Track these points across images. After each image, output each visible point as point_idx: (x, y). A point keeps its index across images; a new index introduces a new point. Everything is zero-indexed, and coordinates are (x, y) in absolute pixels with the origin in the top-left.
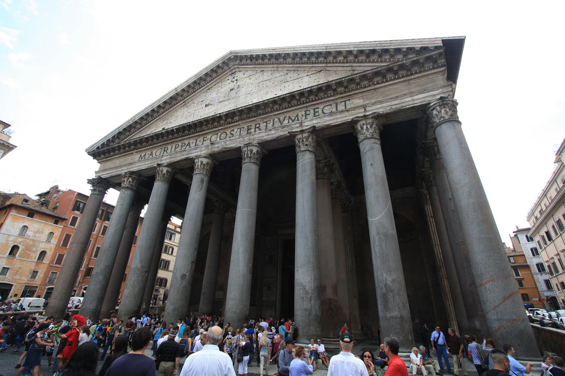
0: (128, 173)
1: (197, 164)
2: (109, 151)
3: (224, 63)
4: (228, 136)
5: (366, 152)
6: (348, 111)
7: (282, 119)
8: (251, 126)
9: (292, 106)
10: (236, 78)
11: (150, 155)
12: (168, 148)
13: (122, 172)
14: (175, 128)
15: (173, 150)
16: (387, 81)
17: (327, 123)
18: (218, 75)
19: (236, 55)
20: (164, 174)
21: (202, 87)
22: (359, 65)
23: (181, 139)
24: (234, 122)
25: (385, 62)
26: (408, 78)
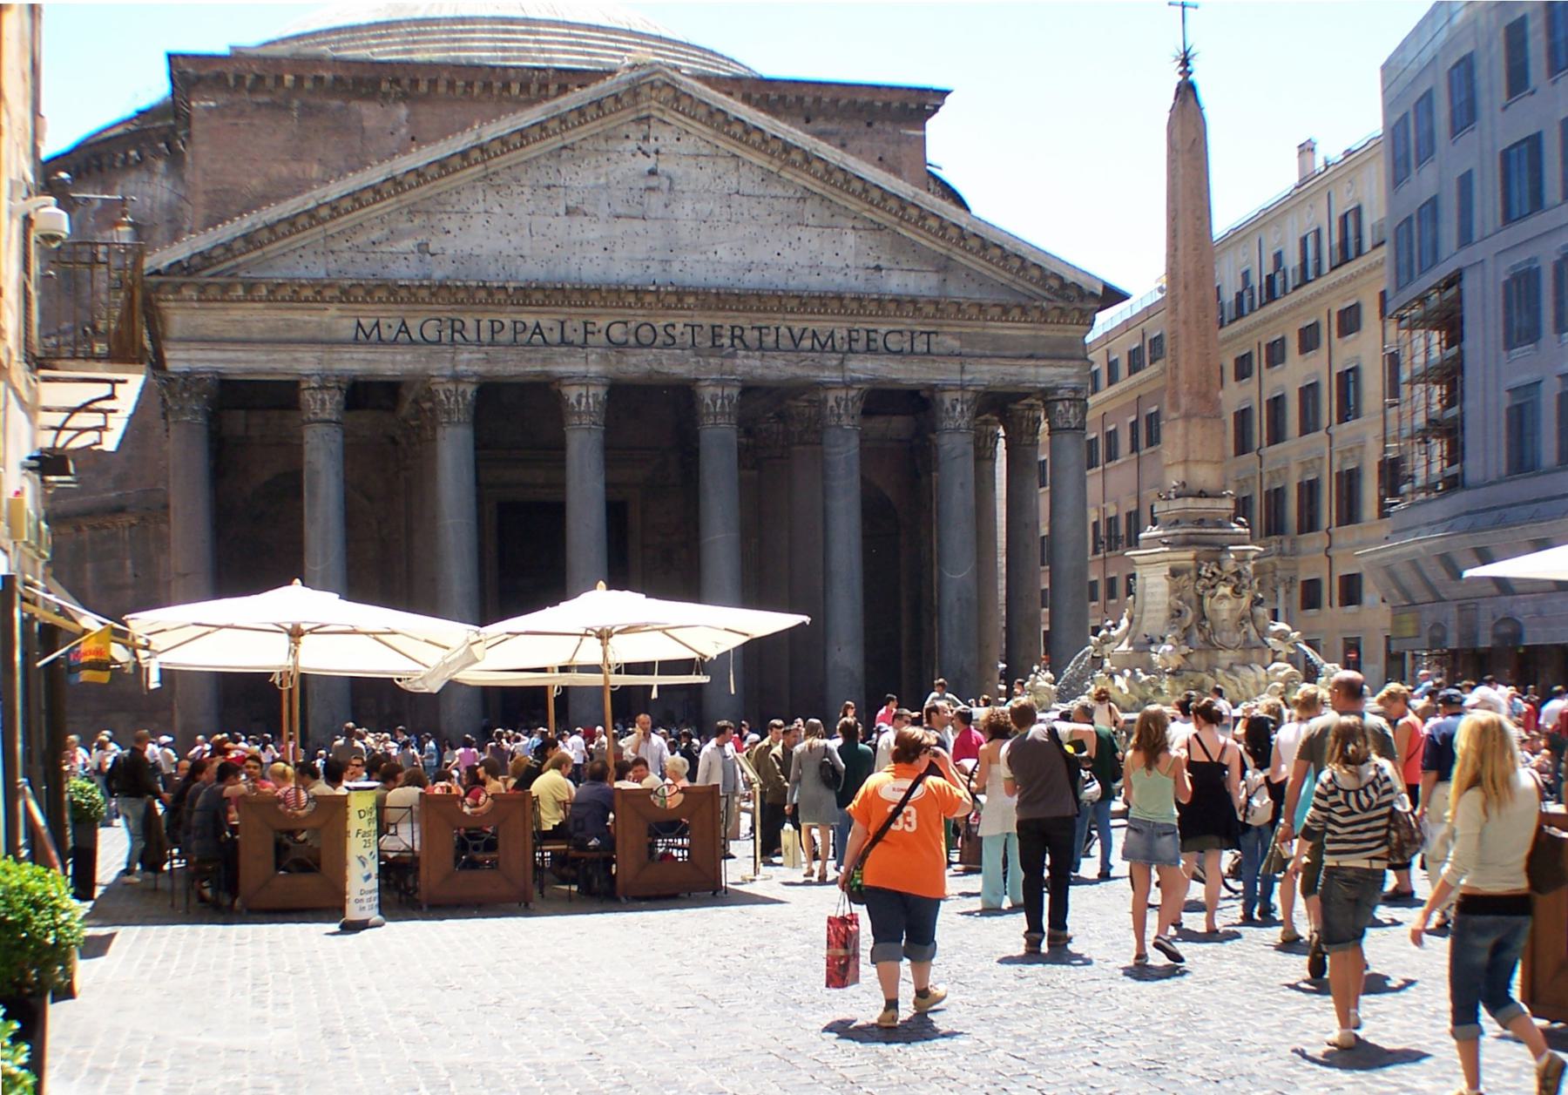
1: (584, 400)
4: (659, 338)
6: (934, 361)
7: (797, 332)
8: (721, 327)
11: (400, 331)
12: (463, 323)
13: (297, 366)
14: (512, 284)
16: (1007, 321)
17: (894, 376)
21: (549, 136)
22: (963, 253)
23: (512, 308)
24: (682, 308)
25: (1010, 271)
26: (1036, 325)
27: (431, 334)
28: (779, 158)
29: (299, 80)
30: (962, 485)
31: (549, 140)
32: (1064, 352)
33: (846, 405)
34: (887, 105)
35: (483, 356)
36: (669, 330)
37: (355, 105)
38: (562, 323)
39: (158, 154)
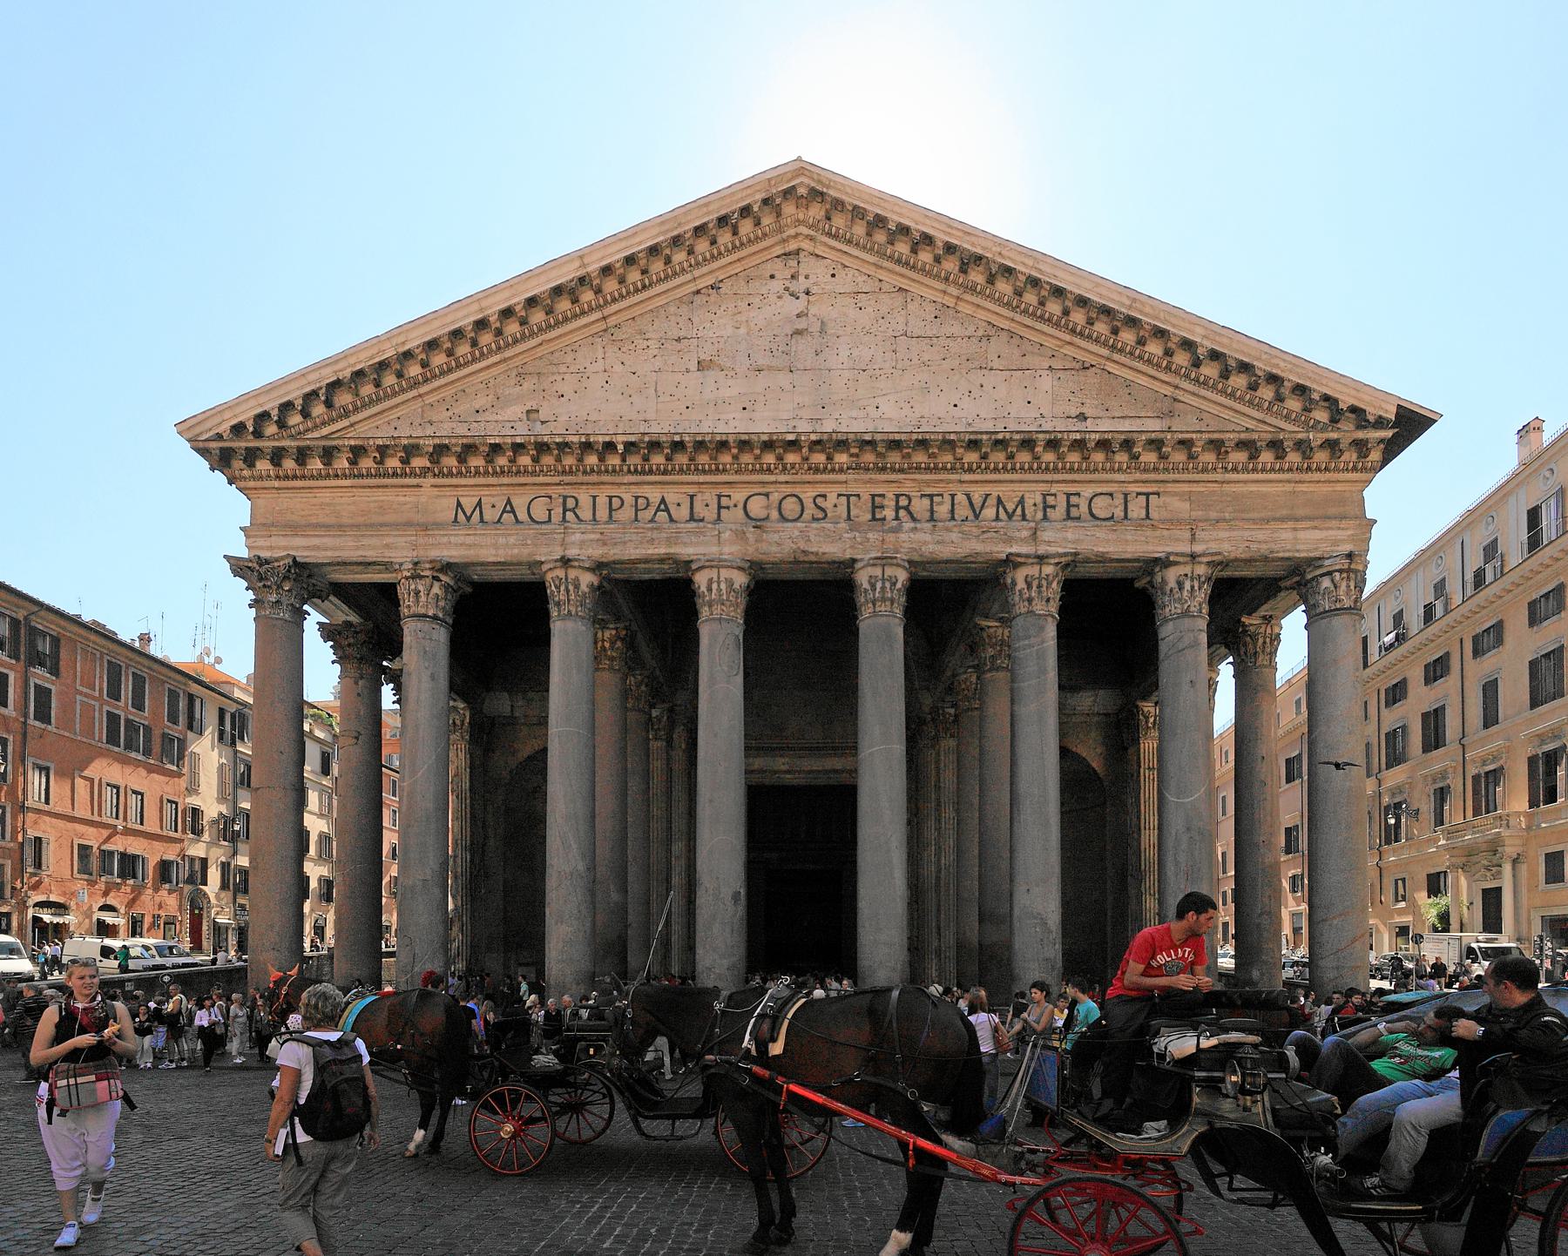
0: (428, 566)
1: (715, 586)
3: (765, 202)
7: (977, 494)
8: (883, 496)
10: (801, 284)
15: (602, 513)
17: (1101, 549)
18: (738, 244)
19: (819, 188)
20: (585, 594)
24: (833, 470)
25: (1259, 407)
27: (539, 512)
28: (955, 283)
31: (678, 281)
32: (1332, 511)
33: (1039, 586)
35: (598, 536)
36: (819, 500)
38: (692, 497)
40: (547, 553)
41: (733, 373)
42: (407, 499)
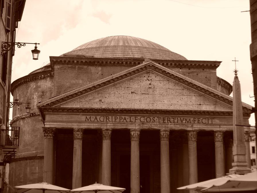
1: (135, 134)
2: (59, 109)
3: (144, 67)
5: (219, 147)
7: (182, 119)
8: (165, 118)
9: (188, 115)
10: (150, 78)
11: (95, 119)
13: (73, 126)
14: (119, 109)
15: (114, 120)
16: (230, 116)
19: (154, 65)
20: (110, 135)
24: (156, 114)
28: (178, 81)
29: (78, 62)
30: (220, 153)
33: (193, 136)
34: (207, 65)
36: (154, 118)
37: (90, 67)
38: (130, 117)
39: (48, 77)
40: (104, 127)
41: (137, 94)
42: (76, 116)
